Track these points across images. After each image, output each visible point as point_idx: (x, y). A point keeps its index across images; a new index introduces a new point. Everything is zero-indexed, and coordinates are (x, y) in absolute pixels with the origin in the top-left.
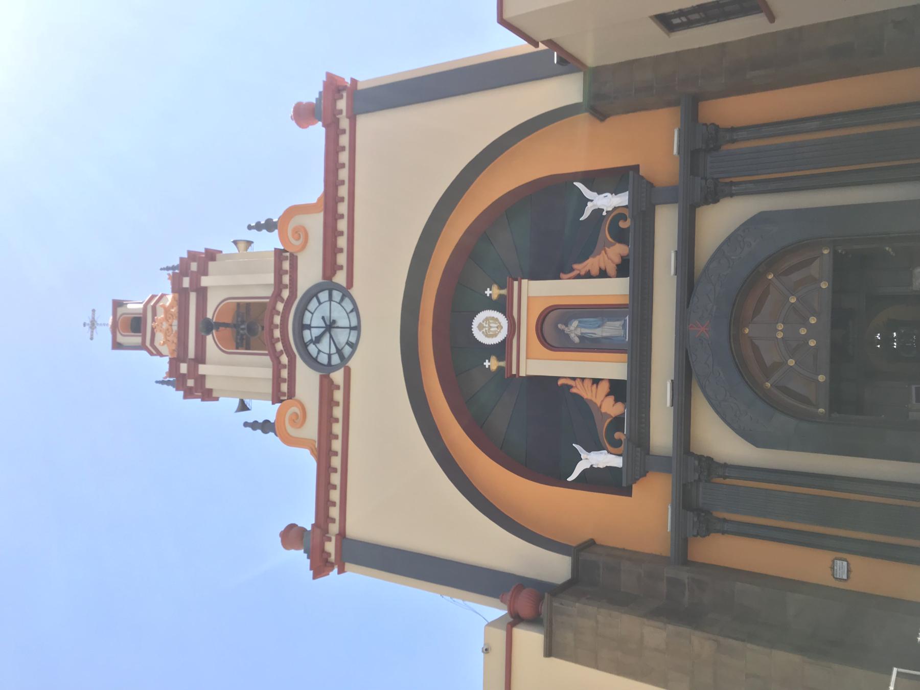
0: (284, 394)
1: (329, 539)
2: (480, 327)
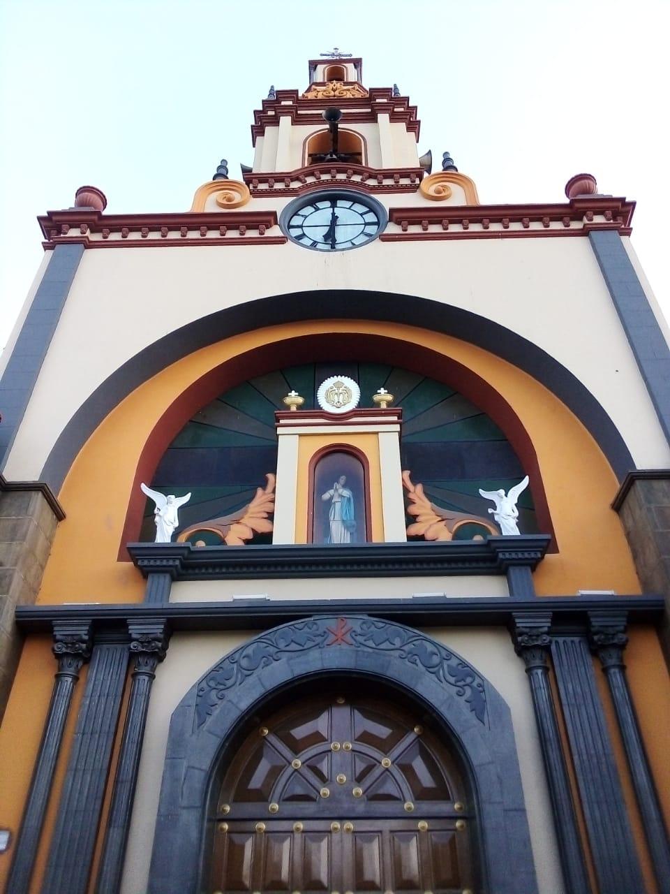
0: (255, 187)
2: (338, 385)
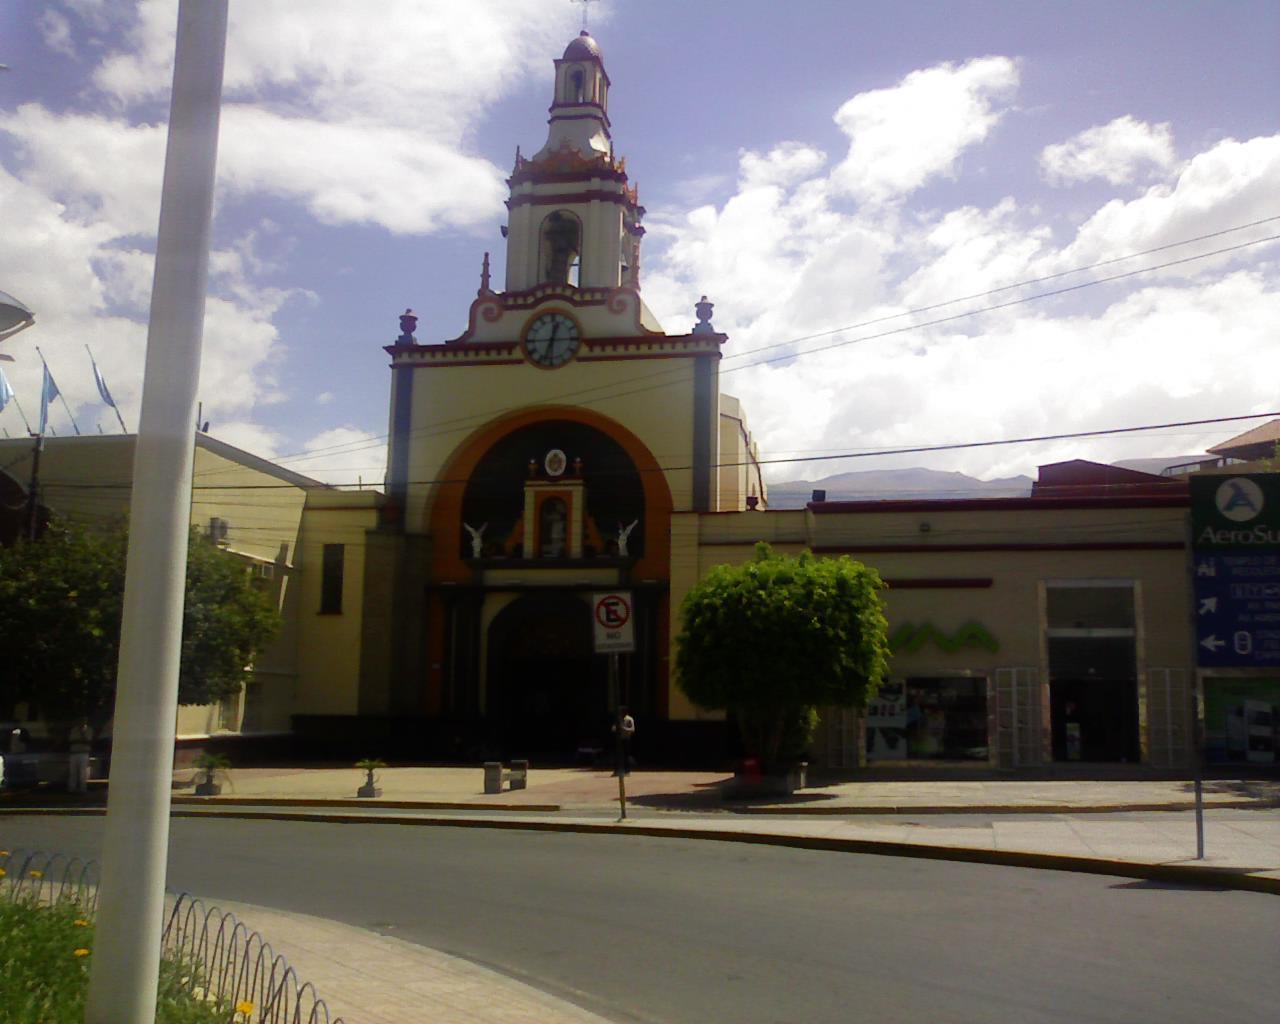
1: (410, 356)
2: (556, 456)
